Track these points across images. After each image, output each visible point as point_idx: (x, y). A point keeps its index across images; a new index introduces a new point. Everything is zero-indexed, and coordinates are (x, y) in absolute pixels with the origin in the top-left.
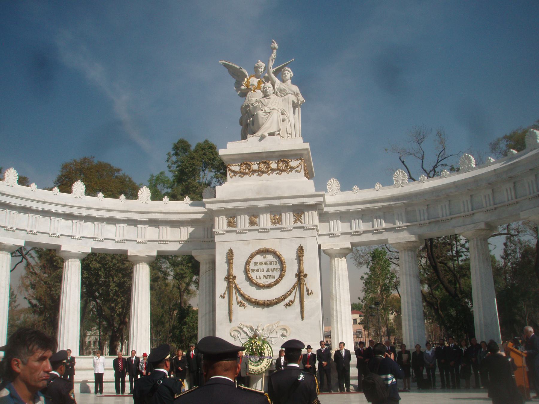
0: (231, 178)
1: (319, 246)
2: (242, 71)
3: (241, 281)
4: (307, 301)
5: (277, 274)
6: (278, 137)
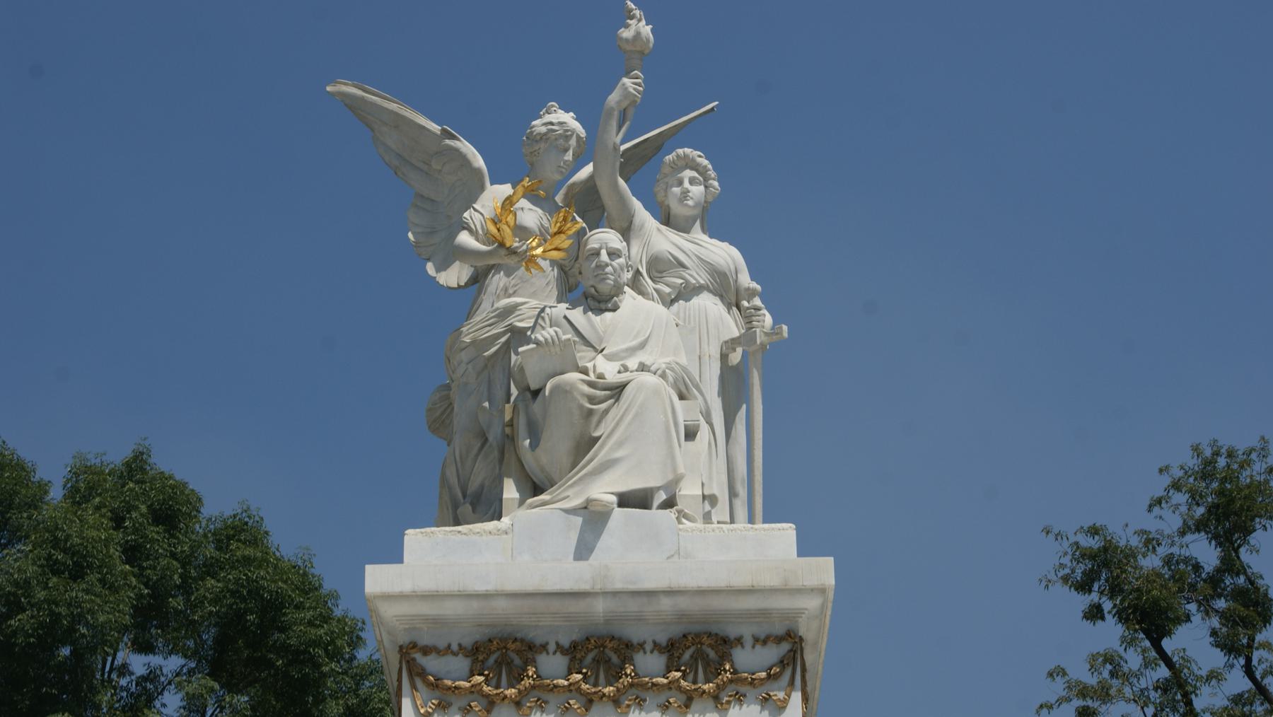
2: (457, 150)
6: (670, 514)
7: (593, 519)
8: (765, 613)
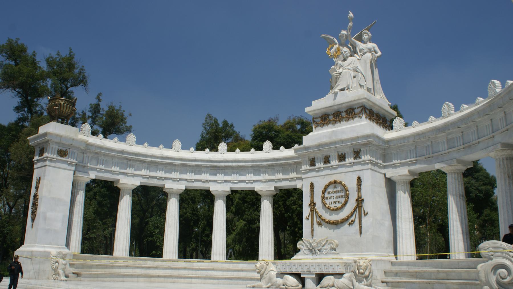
0: (316, 128)
1: (385, 175)
3: (319, 206)
4: (364, 220)
5: (343, 200)
6: (347, 91)
7: (336, 94)
8: (358, 103)
